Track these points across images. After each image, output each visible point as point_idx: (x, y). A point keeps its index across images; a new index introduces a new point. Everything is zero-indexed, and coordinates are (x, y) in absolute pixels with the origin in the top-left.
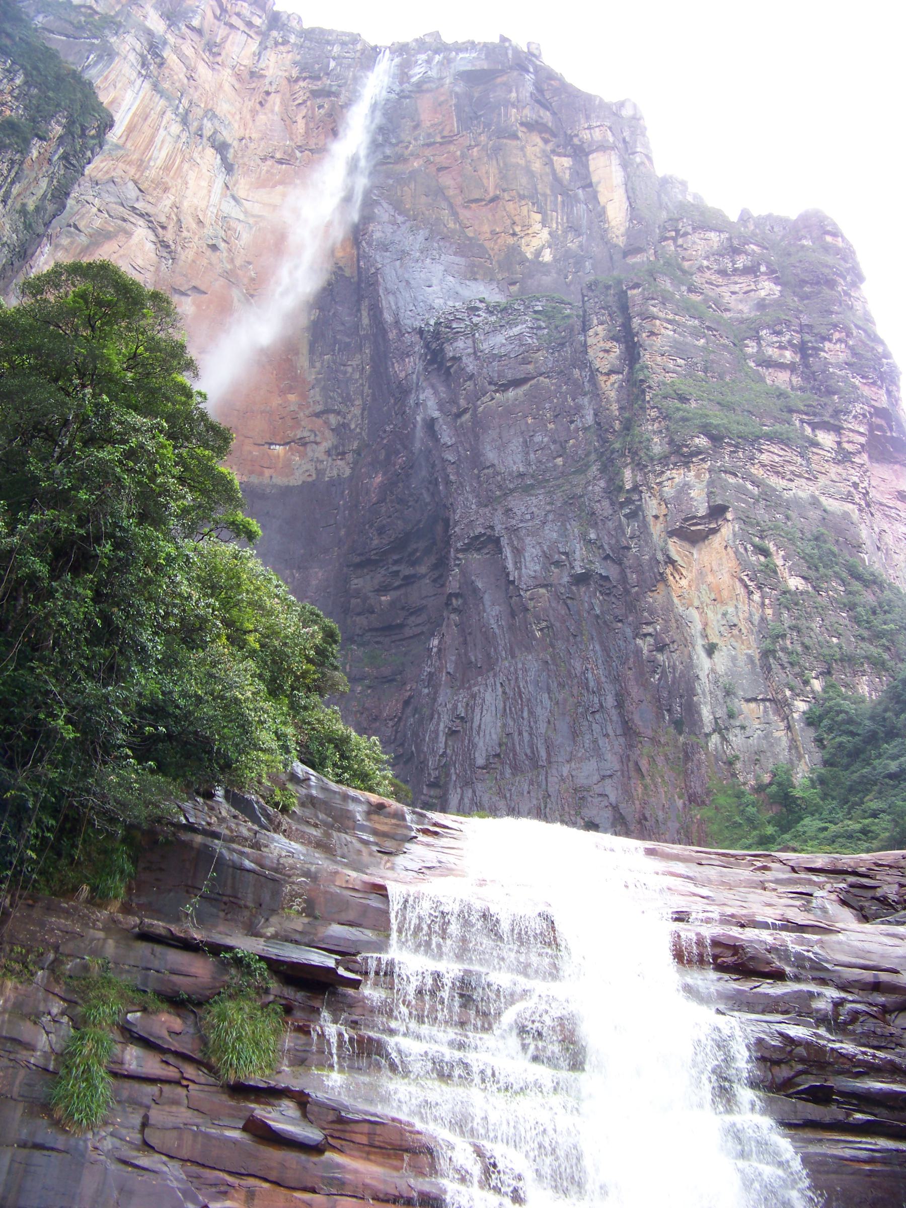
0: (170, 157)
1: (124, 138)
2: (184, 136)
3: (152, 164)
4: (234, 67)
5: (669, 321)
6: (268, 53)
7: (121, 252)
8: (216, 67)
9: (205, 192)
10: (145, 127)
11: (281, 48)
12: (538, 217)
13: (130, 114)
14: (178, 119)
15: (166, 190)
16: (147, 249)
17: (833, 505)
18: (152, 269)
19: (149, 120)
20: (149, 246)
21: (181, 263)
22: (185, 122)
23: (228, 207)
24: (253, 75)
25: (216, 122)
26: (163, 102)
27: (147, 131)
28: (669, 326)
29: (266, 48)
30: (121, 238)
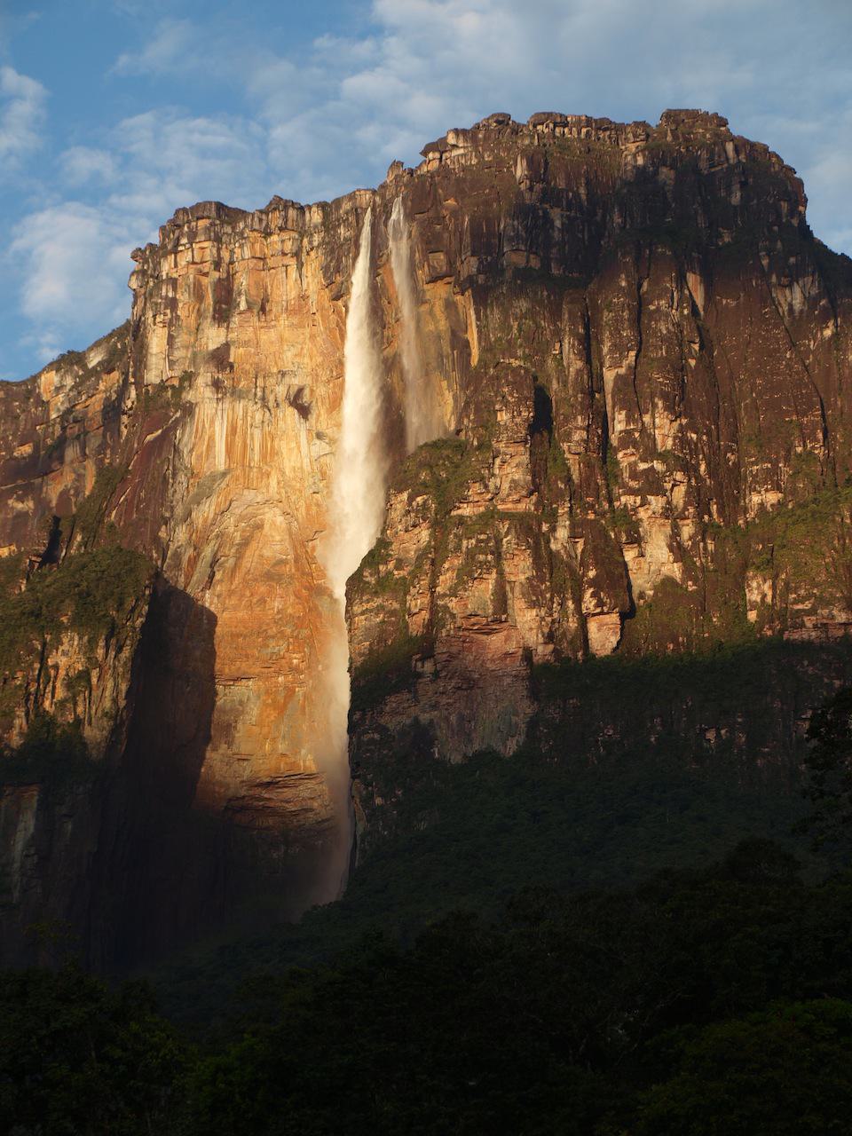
0: (263, 446)
1: (227, 463)
2: (268, 414)
3: (252, 465)
4: (287, 309)
5: (363, 613)
6: (304, 270)
7: (260, 545)
8: (273, 323)
9: (296, 451)
10: (237, 439)
11: (313, 254)
12: (445, 384)
13: (224, 436)
14: (259, 405)
15: (268, 475)
16: (278, 523)
17: (425, 718)
18: (287, 537)
19: (238, 430)
20: (280, 519)
21: (300, 520)
22: (265, 406)
23: (320, 447)
24: (303, 297)
25: (287, 379)
26: (240, 407)
27: (238, 441)
28: (363, 617)
29: (302, 265)
30: (258, 534)
